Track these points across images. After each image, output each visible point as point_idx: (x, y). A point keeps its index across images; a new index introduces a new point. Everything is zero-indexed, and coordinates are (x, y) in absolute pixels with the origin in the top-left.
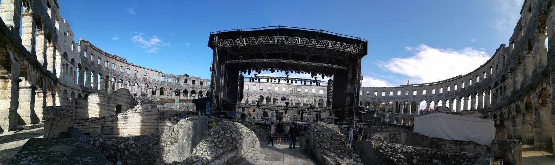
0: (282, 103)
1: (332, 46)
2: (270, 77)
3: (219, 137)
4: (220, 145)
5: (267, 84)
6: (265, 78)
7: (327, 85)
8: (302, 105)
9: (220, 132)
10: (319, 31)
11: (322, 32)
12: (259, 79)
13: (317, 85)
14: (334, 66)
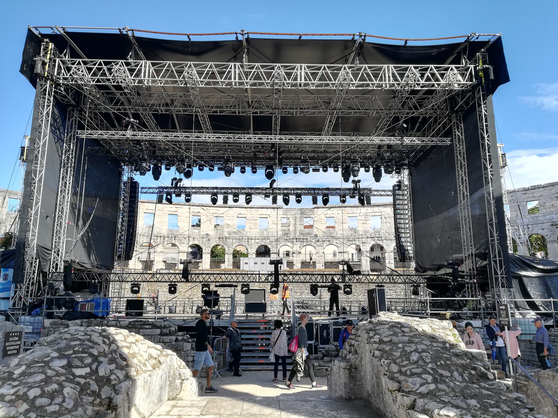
0: (259, 263)
1: (396, 80)
2: (222, 188)
3: (47, 381)
4: (50, 405)
5: (213, 210)
6: (207, 193)
7: (390, 200)
9: (51, 364)
10: (357, 38)
11: (364, 40)
12: (188, 195)
13: (362, 202)
14: (407, 140)
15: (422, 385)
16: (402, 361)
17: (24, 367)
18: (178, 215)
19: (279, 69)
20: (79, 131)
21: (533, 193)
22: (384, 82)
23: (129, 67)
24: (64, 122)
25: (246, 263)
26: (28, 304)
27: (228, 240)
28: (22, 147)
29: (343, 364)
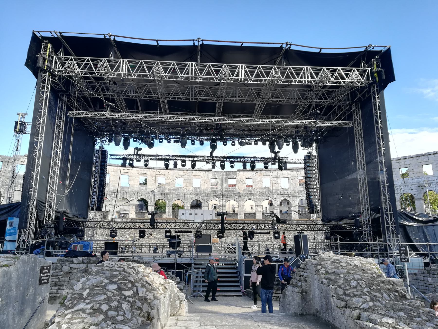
1: (312, 77)
2: (173, 156)
3: (108, 300)
4: (118, 316)
5: (166, 172)
6: (162, 159)
7: (303, 166)
8: (259, 217)
9: (107, 288)
10: (284, 46)
11: (290, 48)
12: (147, 161)
13: (280, 168)
14: (320, 123)
15: (363, 303)
16: (345, 287)
17: (88, 290)
18: (129, 175)
19: (225, 69)
20: (69, 112)
21: (404, 162)
22: (303, 79)
23: (110, 63)
24: (56, 103)
25: (183, 214)
26: (29, 246)
27: (169, 196)
28: (15, 122)
29: (297, 290)
